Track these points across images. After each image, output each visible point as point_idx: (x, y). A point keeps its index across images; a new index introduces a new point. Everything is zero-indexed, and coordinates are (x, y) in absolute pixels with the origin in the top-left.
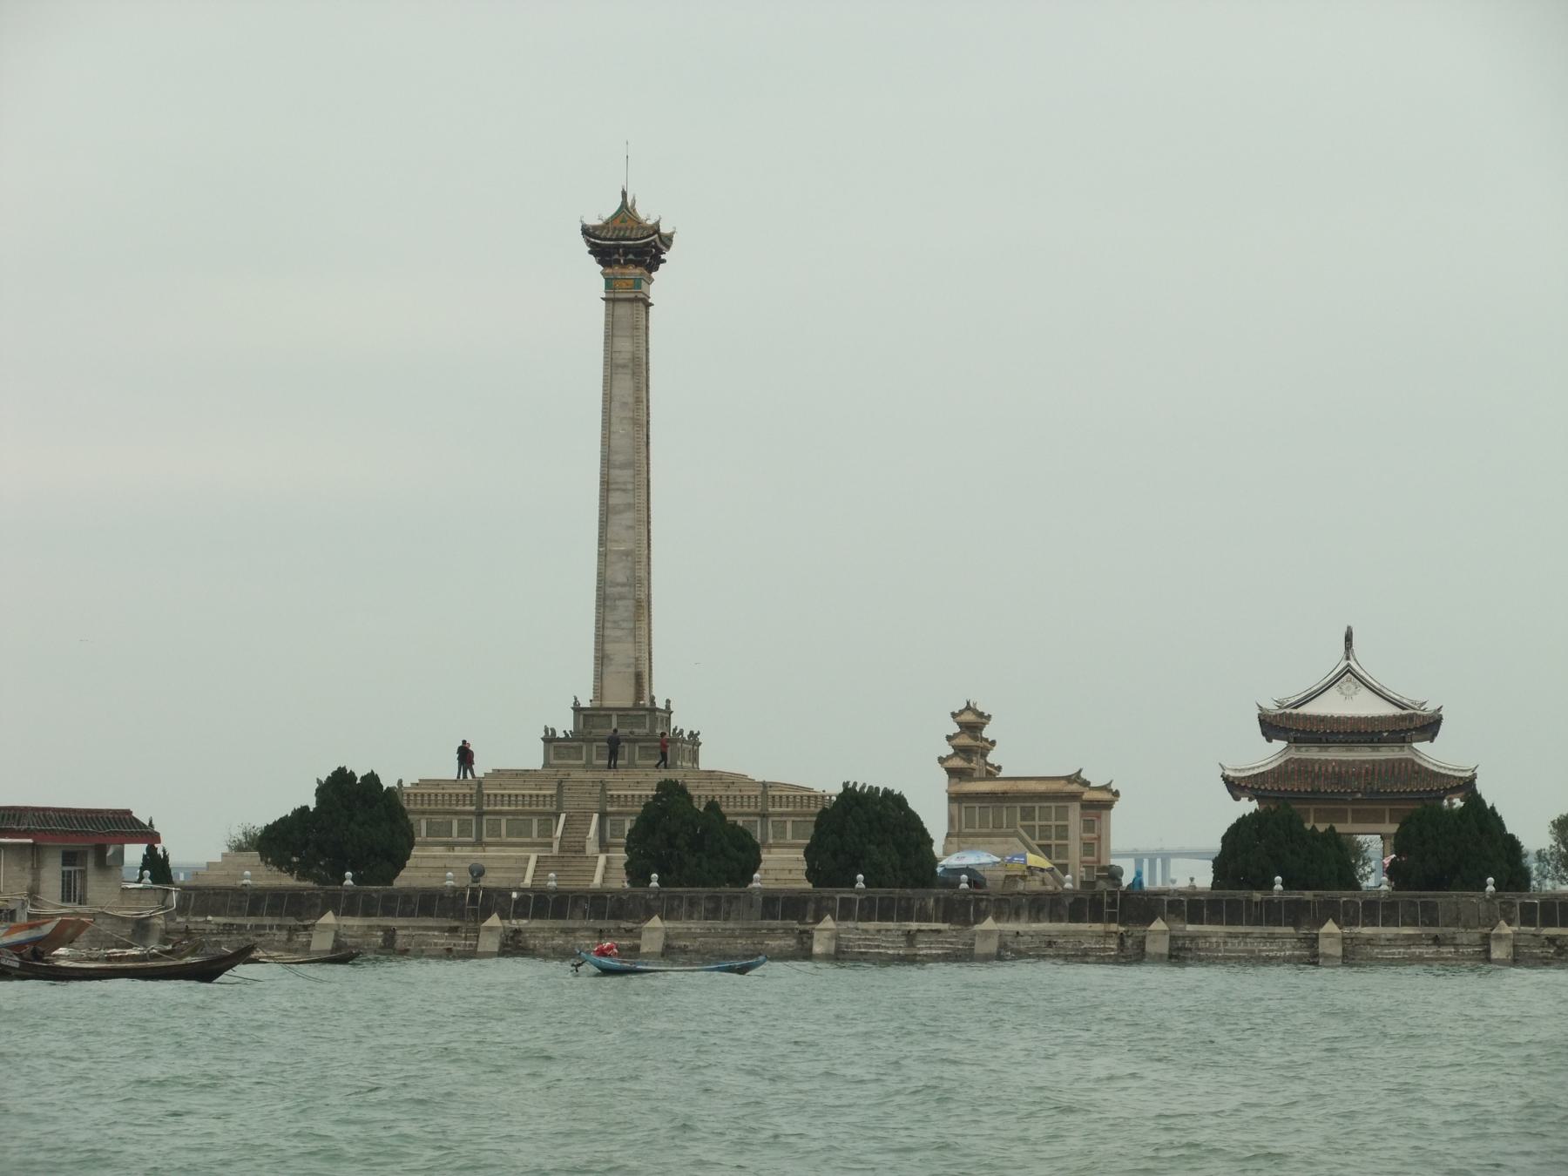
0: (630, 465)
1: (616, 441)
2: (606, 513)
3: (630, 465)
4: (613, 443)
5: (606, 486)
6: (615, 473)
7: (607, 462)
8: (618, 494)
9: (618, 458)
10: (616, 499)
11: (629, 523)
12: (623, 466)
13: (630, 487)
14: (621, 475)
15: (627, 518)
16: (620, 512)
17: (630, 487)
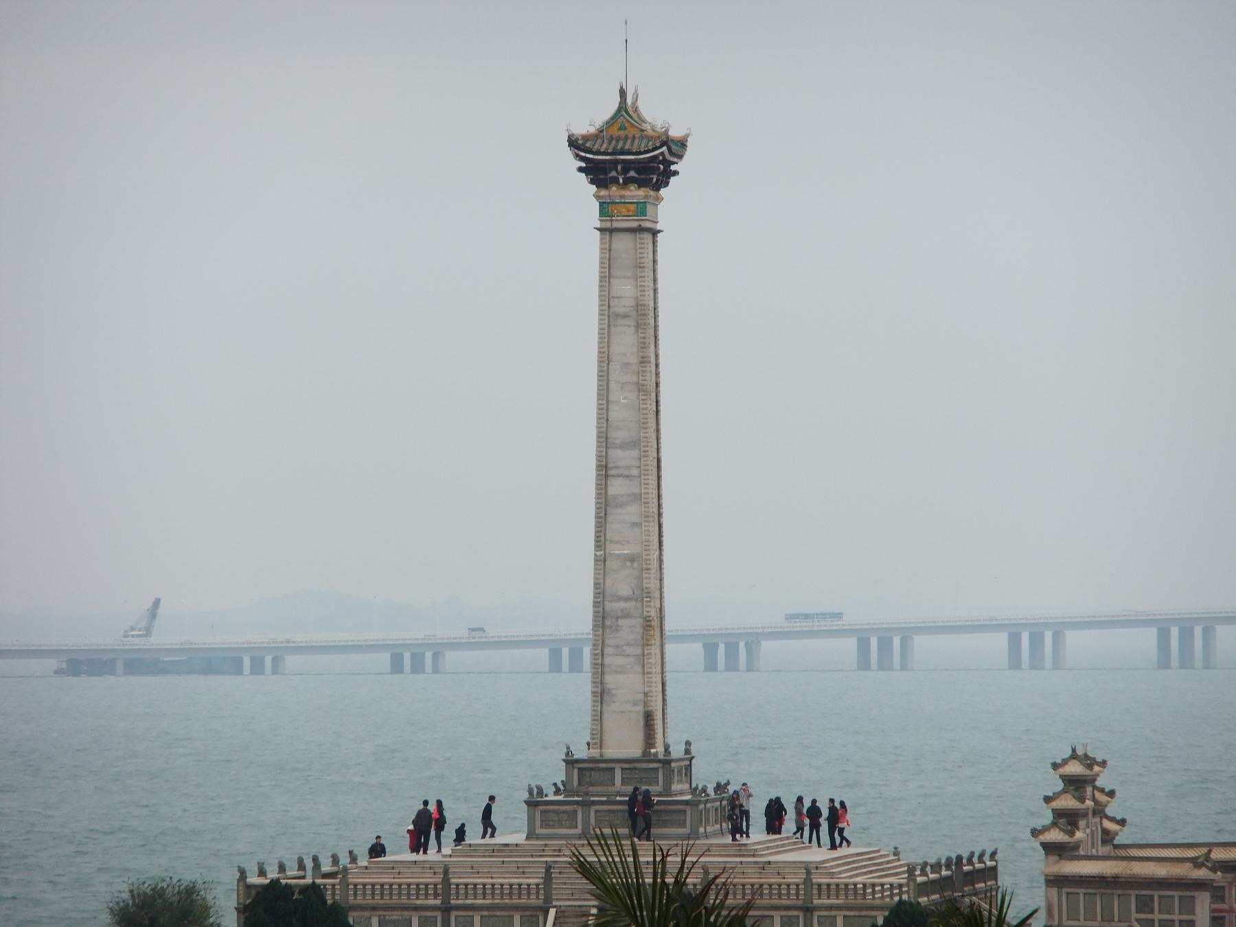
0: (635, 444)
1: (616, 413)
2: (604, 506)
3: (635, 444)
4: (612, 415)
5: (604, 471)
6: (615, 454)
7: (605, 441)
8: (619, 481)
9: (619, 436)
10: (617, 487)
11: (635, 519)
12: (624, 446)
13: (635, 472)
14: (620, 457)
15: (632, 512)
16: (621, 506)
17: (635, 472)
